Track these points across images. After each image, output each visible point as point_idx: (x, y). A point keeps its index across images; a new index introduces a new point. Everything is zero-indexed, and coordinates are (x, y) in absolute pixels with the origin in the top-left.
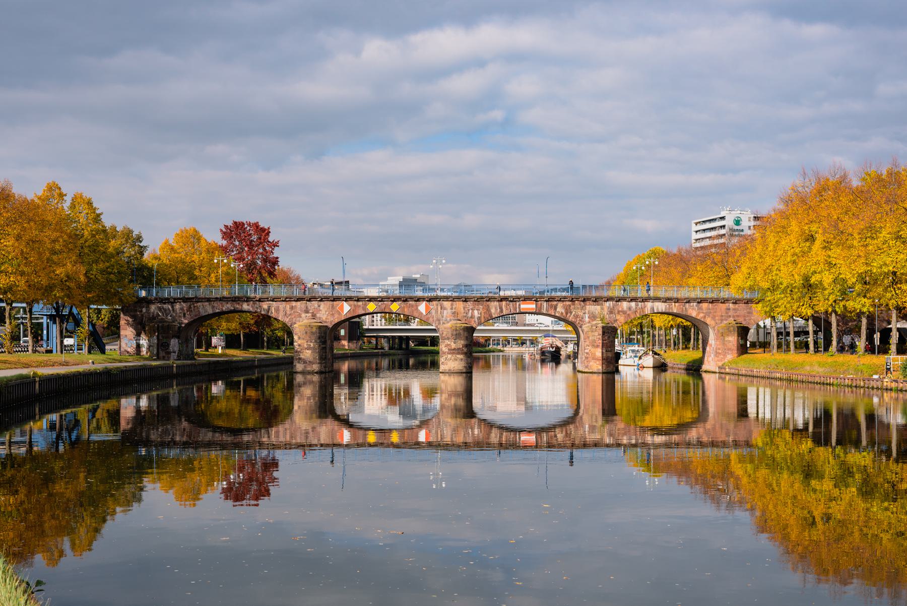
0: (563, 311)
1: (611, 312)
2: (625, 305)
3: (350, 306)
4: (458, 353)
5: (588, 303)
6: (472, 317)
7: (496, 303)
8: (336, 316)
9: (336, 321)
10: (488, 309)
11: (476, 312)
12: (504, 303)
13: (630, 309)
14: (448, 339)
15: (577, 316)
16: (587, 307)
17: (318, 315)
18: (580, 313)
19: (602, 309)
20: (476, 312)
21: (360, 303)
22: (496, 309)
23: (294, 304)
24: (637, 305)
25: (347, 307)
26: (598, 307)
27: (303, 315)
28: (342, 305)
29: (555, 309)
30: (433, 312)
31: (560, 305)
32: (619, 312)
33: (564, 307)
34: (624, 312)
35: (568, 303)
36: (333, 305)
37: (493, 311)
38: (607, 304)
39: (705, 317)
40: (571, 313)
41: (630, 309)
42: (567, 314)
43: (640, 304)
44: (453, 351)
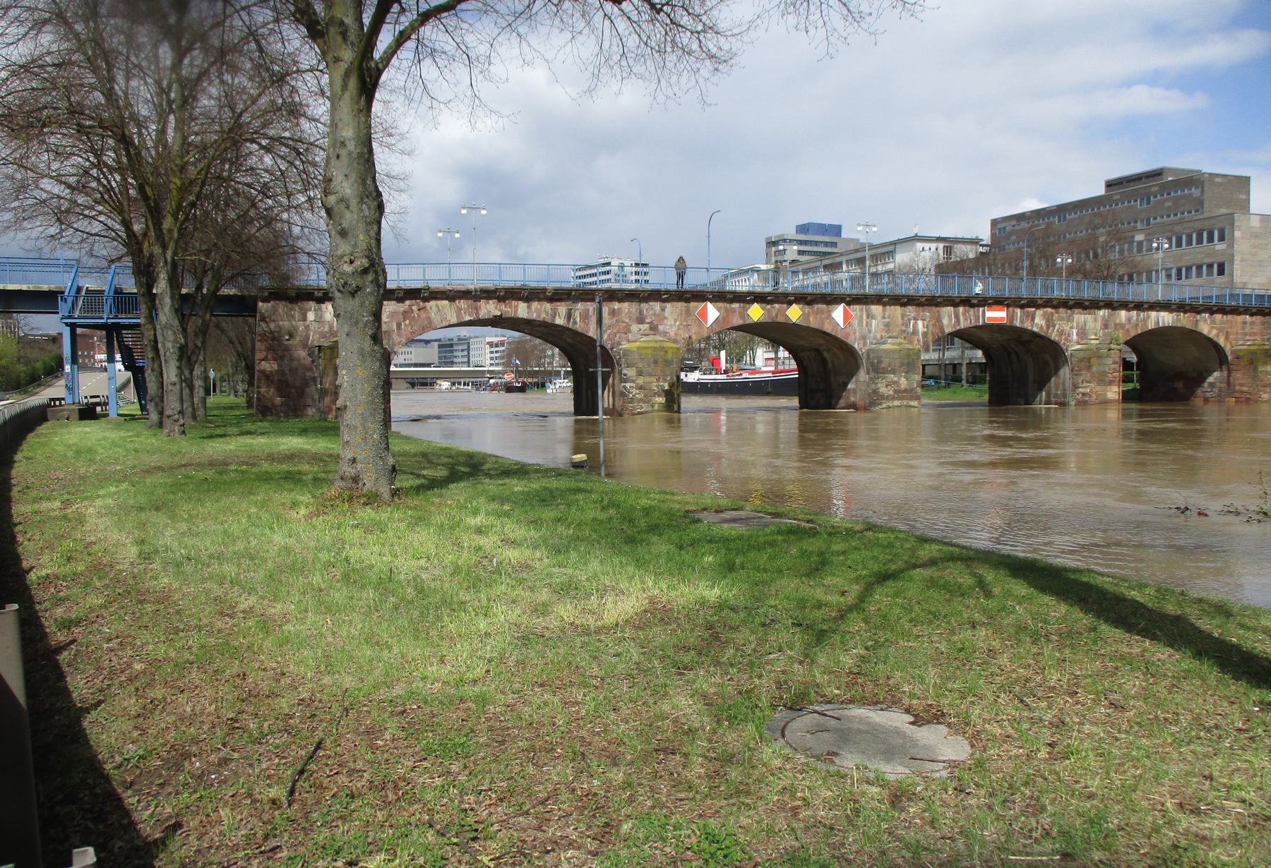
0: (1043, 323)
3: (718, 309)
6: (915, 332)
7: (951, 309)
11: (920, 323)
12: (961, 309)
14: (893, 372)
15: (1061, 333)
16: (1076, 316)
17: (661, 328)
18: (1067, 328)
19: (1096, 320)
20: (920, 323)
21: (736, 305)
22: (950, 319)
23: (616, 305)
25: (713, 312)
26: (1089, 317)
27: (635, 328)
28: (705, 310)
29: (1033, 319)
30: (855, 323)
31: (1039, 313)
34: (1122, 326)
37: (945, 321)
39: (1218, 335)
40: (1054, 326)
41: (1129, 320)
42: (1048, 328)
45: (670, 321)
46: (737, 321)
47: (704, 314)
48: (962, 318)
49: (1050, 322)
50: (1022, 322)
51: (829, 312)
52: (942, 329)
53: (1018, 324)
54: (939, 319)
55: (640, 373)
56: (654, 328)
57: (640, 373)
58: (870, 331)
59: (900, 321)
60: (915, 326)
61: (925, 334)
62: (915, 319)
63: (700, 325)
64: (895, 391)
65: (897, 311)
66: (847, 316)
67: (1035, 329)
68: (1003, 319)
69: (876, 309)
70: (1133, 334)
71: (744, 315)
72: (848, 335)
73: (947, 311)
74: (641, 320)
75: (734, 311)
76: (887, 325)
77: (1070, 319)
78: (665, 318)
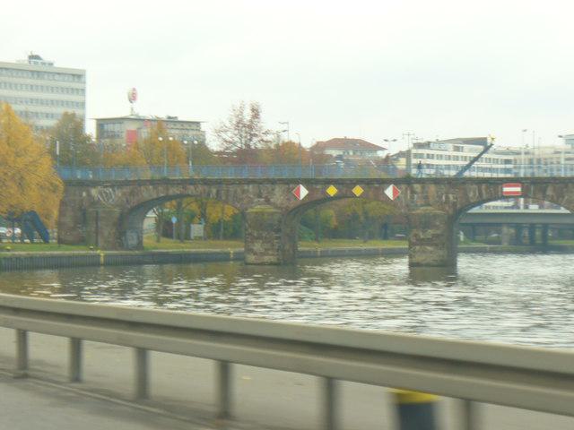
4: (428, 245)
7: (475, 186)
12: (484, 186)
17: (272, 200)
23: (246, 187)
37: (471, 195)
40: (563, 197)
51: (384, 189)
54: (466, 194)
55: (250, 226)
56: (268, 201)
57: (250, 226)
58: (413, 202)
60: (447, 197)
62: (447, 193)
64: (417, 240)
66: (395, 192)
74: (260, 196)
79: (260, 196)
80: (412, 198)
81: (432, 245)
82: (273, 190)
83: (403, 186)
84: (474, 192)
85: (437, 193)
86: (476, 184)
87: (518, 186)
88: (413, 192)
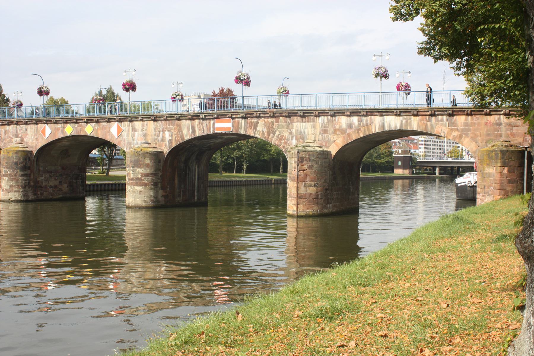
0: (265, 130)
1: (325, 131)
2: (343, 121)
4: (137, 184)
5: (295, 119)
7: (189, 122)
8: (40, 140)
9: (40, 145)
10: (180, 129)
11: (167, 133)
12: (197, 121)
13: (350, 126)
15: (281, 138)
16: (295, 124)
17: (25, 139)
18: (286, 134)
19: (314, 127)
20: (167, 133)
21: (60, 126)
22: (188, 131)
23: (7, 127)
24: (360, 121)
26: (309, 125)
27: (14, 139)
28: (44, 129)
30: (124, 134)
31: (261, 122)
32: (335, 131)
33: (265, 124)
34: (343, 131)
35: (270, 120)
36: (37, 131)
37: (185, 132)
38: (321, 120)
40: (274, 133)
41: (350, 126)
43: (364, 119)
44: (137, 181)
45: (29, 136)
46: (60, 136)
47: (44, 131)
48: (197, 129)
49: (271, 130)
50: (245, 130)
51: (110, 128)
52: (182, 137)
53: (242, 132)
58: (134, 140)
59: (153, 133)
61: (170, 141)
62: (164, 131)
63: (42, 138)
65: (151, 125)
66: (119, 130)
67: (257, 135)
68: (229, 128)
69: (138, 124)
70: (354, 137)
71: (63, 132)
72: (120, 142)
73: (186, 124)
75: (58, 129)
76: (145, 135)
77: (288, 126)
78: (27, 134)
79: (17, 136)
80: (133, 135)
81: (141, 185)
82: (26, 130)
83: (126, 123)
84: (188, 128)
85: (155, 129)
86: (190, 119)
87: (228, 122)
88: (134, 130)
